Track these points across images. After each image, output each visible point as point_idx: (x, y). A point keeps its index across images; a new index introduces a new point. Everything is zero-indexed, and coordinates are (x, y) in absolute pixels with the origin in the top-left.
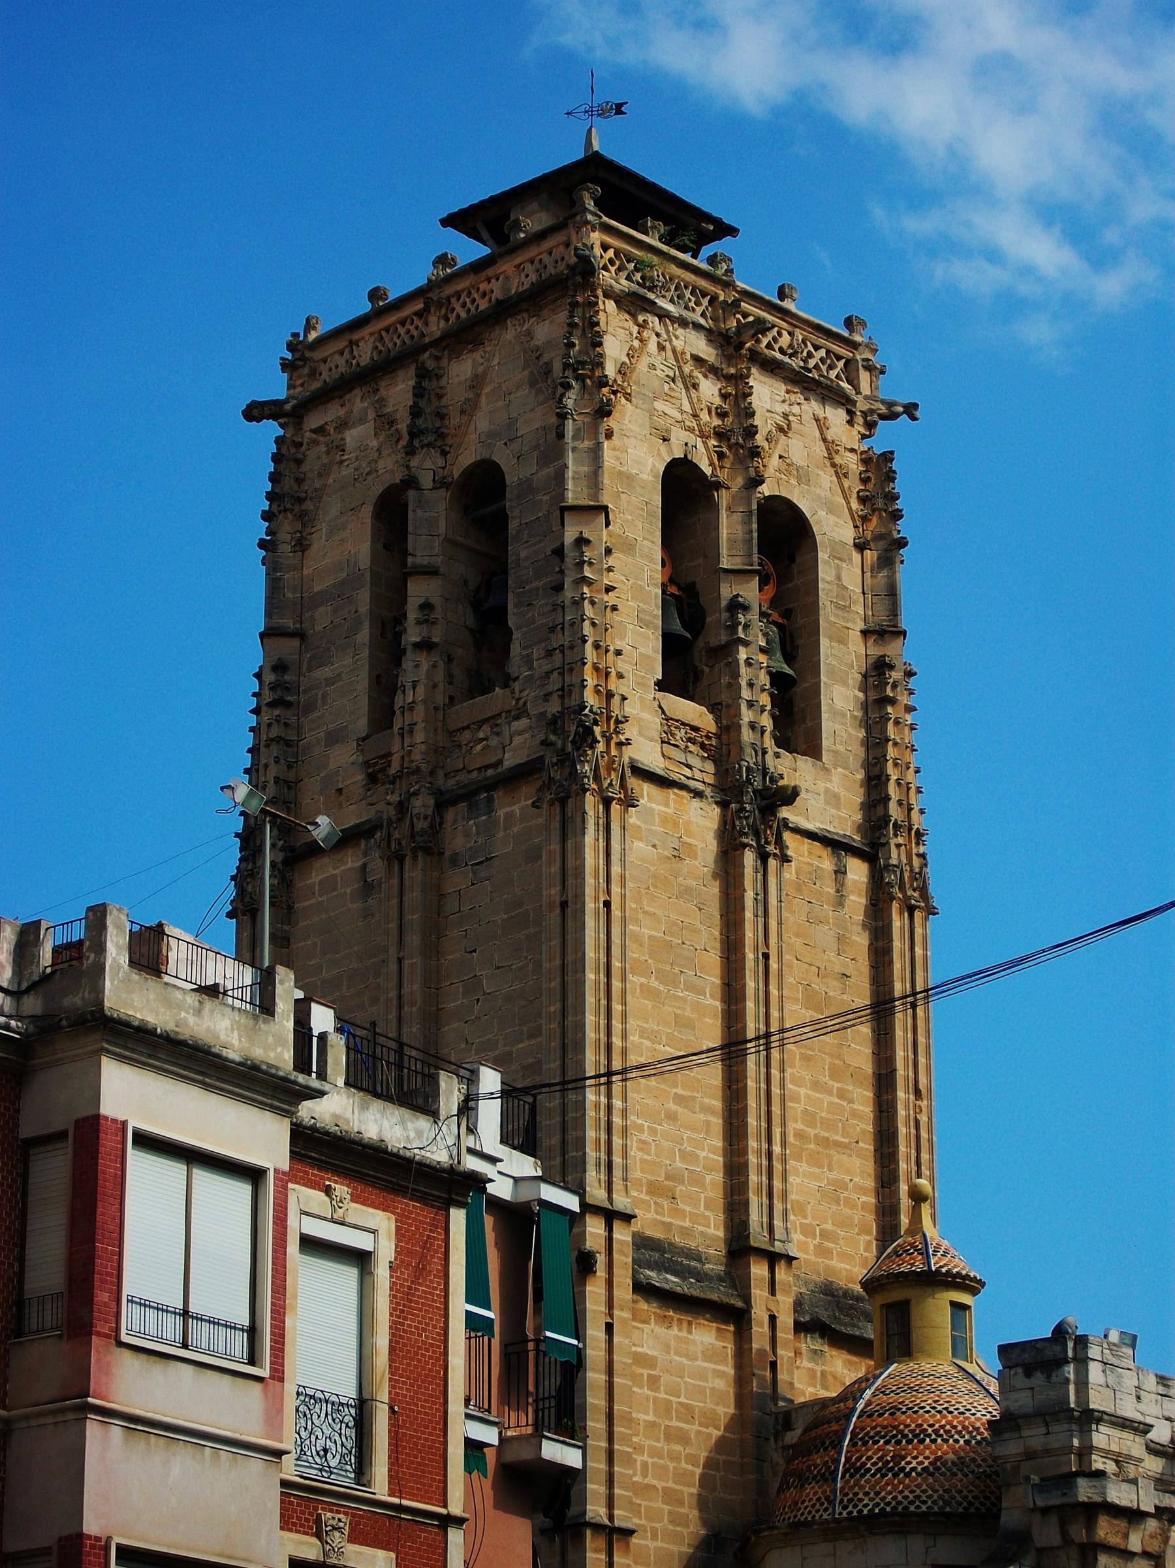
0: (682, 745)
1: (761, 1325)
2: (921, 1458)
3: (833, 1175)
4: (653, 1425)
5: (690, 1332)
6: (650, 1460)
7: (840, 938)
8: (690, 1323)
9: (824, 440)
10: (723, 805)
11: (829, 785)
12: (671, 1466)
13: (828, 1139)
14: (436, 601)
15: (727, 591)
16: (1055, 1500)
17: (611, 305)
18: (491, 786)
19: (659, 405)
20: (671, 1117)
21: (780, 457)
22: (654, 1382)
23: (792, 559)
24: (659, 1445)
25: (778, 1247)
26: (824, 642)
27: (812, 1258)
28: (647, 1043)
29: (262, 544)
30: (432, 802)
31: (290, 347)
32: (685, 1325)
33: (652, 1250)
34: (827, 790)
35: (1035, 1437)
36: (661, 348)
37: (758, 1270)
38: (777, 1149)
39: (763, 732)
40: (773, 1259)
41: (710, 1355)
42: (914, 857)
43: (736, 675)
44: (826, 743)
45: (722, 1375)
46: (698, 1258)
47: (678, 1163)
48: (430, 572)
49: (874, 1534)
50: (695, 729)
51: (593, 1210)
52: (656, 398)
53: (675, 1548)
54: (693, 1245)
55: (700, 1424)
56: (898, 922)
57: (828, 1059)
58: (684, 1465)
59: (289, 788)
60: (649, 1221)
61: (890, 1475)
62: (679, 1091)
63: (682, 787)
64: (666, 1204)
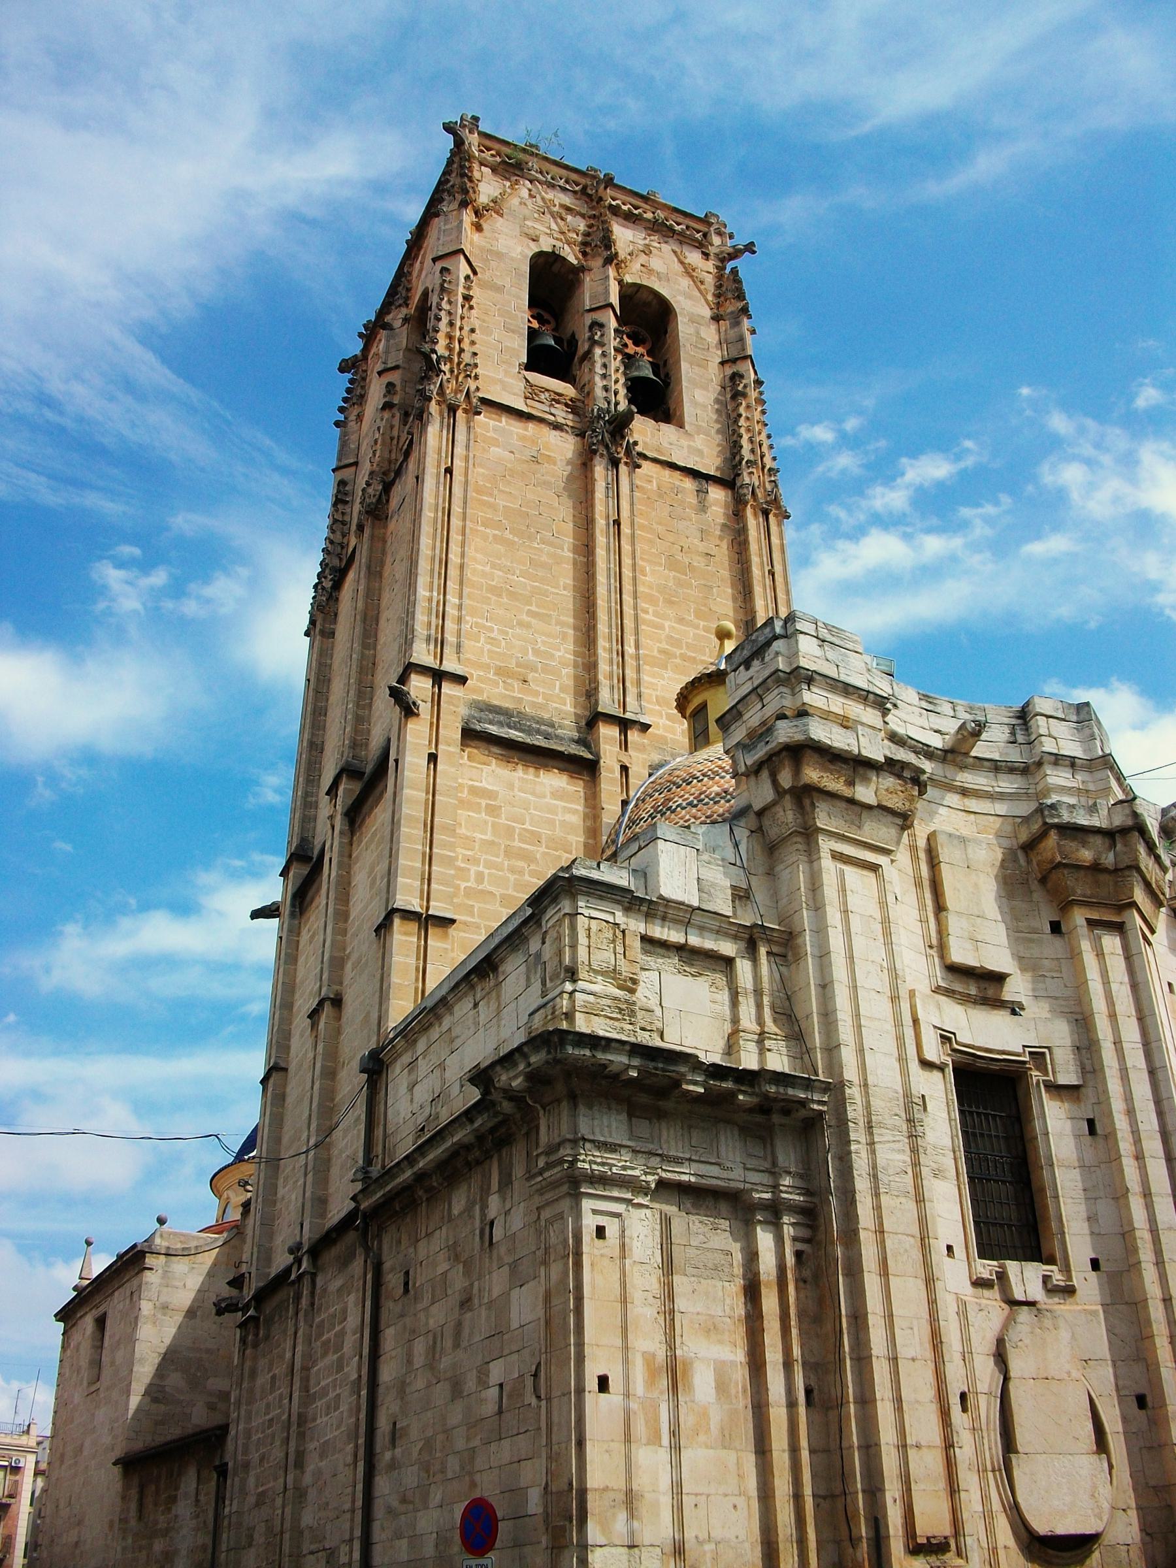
1: (613, 772)
4: (492, 843)
5: (538, 776)
6: (487, 871)
9: (682, 263)
10: (581, 434)
11: (692, 443)
12: (512, 877)
13: (695, 658)
14: (398, 383)
16: (761, 752)
21: (642, 265)
22: (493, 810)
24: (500, 860)
25: (628, 715)
28: (500, 573)
29: (338, 424)
30: (381, 487)
31: (364, 326)
33: (498, 713)
34: (689, 447)
36: (531, 196)
37: (608, 733)
39: (616, 394)
40: (625, 725)
41: (557, 794)
42: (767, 484)
44: (687, 419)
45: (575, 812)
48: (396, 367)
51: (418, 669)
52: (525, 219)
54: (546, 716)
55: (547, 847)
56: (753, 523)
57: (693, 606)
58: (527, 877)
59: (342, 548)
61: (659, 815)
62: (534, 608)
63: (541, 420)
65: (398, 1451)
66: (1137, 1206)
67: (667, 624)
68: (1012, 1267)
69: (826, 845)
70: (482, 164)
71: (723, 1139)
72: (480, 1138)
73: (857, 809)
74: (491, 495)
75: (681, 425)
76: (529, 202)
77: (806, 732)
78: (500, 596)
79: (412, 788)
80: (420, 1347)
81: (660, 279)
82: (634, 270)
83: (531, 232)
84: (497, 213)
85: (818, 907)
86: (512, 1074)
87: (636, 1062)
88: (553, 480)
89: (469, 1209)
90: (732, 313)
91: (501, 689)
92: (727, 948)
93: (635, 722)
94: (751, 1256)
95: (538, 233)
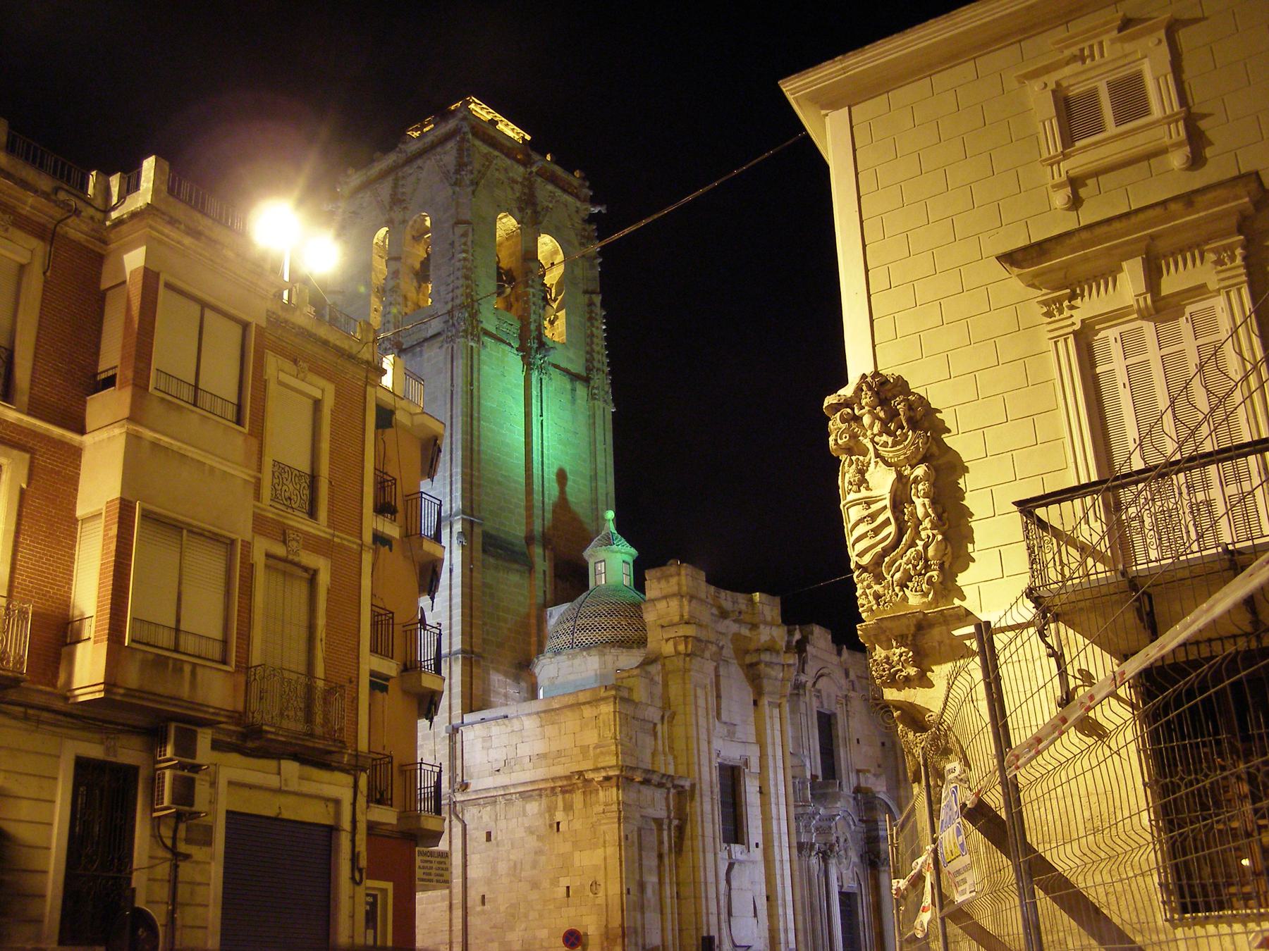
65: (487, 907)
66: (775, 822)
68: (732, 845)
94: (661, 843)
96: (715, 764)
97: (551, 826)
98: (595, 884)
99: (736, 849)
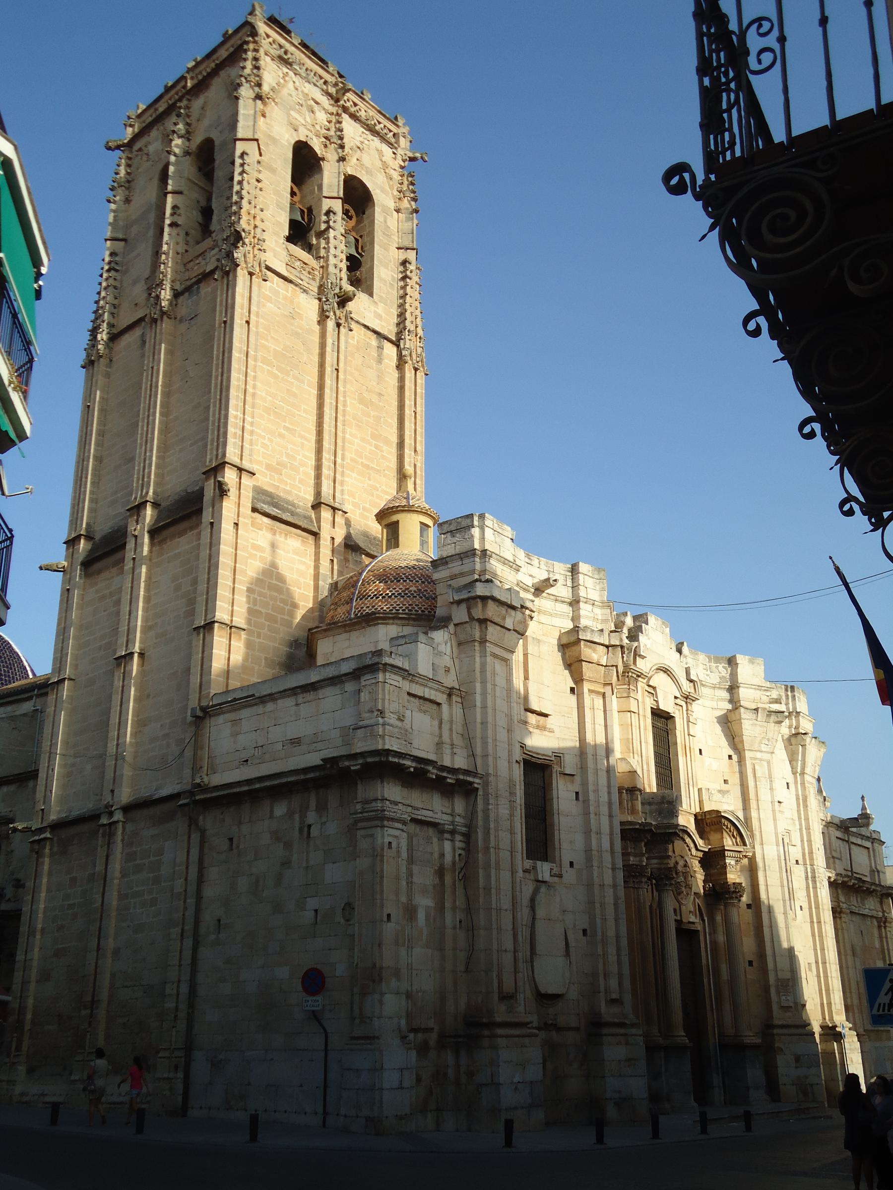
0: (299, 269)
2: (397, 589)
3: (371, 482)
5: (286, 539)
7: (379, 377)
8: (286, 535)
15: (326, 204)
16: (464, 595)
17: (268, 59)
18: (199, 282)
19: (292, 113)
20: (281, 436)
23: (364, 213)
24: (265, 591)
25: (337, 505)
26: (376, 247)
27: (358, 519)
28: (271, 398)
32: (283, 535)
33: (266, 496)
34: (375, 312)
35: (455, 567)
37: (326, 514)
38: (339, 460)
40: (334, 509)
41: (296, 552)
42: (418, 348)
43: (328, 243)
44: (375, 291)
46: (293, 505)
47: (284, 458)
49: (370, 626)
50: (306, 264)
53: (272, 644)
54: (291, 499)
57: (370, 430)
58: (278, 603)
60: (264, 480)
61: (381, 597)
62: (287, 425)
63: (296, 285)
64: (276, 476)
67: (356, 441)
68: (539, 863)
69: (490, 648)
70: (266, 54)
71: (434, 798)
72: (305, 782)
73: (504, 630)
74: (267, 340)
75: (371, 295)
76: (294, 93)
77: (491, 591)
78: (269, 414)
79: (225, 545)
80: (243, 883)
81: (367, 172)
82: (352, 164)
83: (294, 121)
84: (274, 101)
85: (484, 682)
86: (352, 763)
87: (414, 765)
88: (301, 331)
89: (290, 814)
90: (407, 209)
91: (268, 480)
92: (441, 698)
93: (339, 510)
95: (298, 123)
96: (518, 755)
97: (301, 830)
98: (349, 907)
99: (544, 870)
